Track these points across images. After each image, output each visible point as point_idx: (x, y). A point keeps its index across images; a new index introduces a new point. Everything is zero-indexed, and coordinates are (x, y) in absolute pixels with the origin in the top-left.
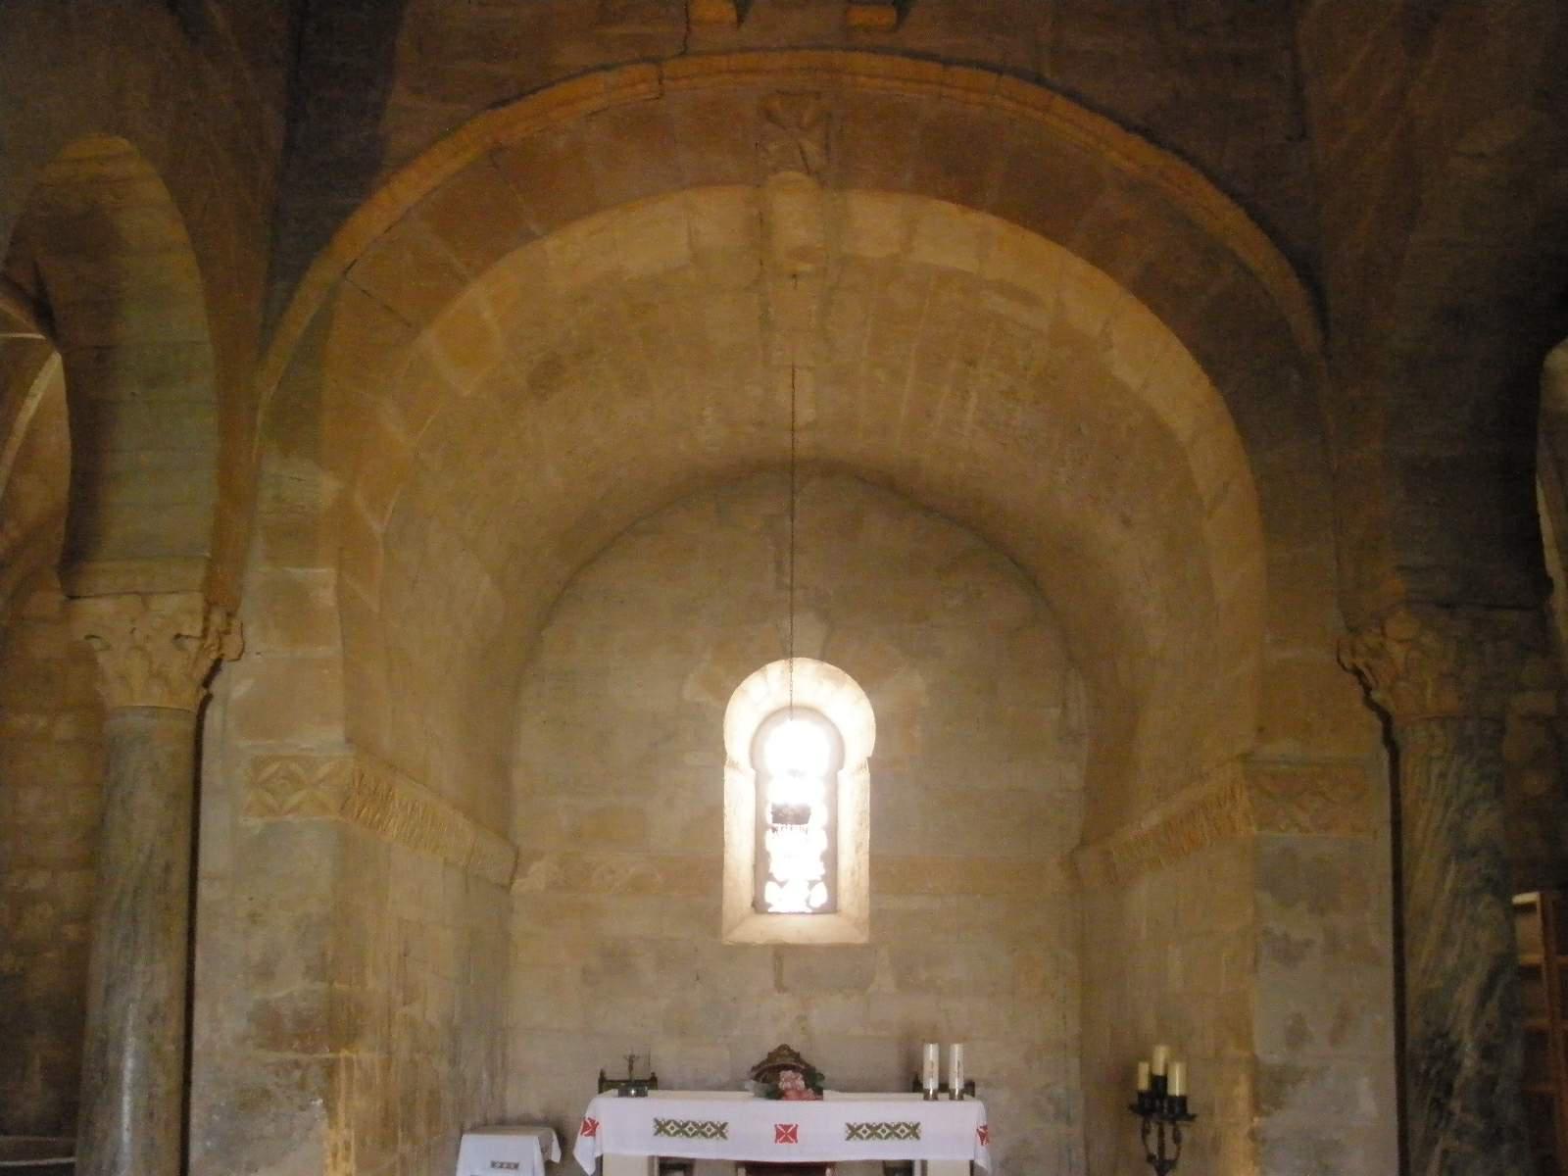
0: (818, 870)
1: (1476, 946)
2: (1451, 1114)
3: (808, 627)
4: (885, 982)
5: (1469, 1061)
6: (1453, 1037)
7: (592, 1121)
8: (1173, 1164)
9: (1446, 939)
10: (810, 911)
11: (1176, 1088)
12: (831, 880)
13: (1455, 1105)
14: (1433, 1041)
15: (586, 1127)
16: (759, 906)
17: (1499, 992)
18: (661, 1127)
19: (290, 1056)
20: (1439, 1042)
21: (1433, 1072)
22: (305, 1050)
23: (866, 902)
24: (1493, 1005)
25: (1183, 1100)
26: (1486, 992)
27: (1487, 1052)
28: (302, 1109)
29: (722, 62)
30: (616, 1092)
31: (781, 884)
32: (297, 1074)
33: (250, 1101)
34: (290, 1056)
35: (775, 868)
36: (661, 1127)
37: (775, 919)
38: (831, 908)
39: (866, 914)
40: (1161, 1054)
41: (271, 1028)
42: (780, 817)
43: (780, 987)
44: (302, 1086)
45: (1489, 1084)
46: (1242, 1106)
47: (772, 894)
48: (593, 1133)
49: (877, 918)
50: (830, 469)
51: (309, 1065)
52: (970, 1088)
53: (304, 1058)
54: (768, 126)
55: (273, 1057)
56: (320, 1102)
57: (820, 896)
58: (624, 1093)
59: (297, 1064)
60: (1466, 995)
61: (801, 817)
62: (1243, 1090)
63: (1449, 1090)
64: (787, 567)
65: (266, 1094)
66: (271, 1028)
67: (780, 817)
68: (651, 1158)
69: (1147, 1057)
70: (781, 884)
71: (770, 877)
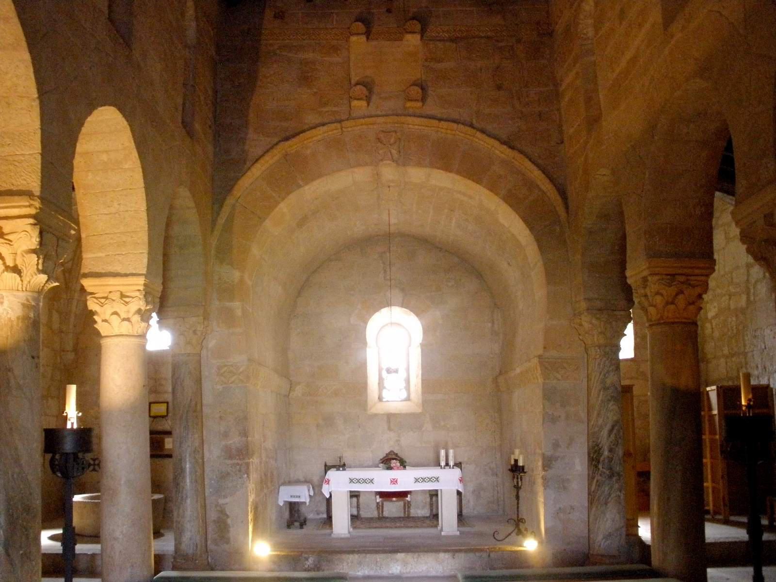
0: (403, 385)
1: (608, 418)
2: (599, 469)
3: (397, 294)
4: (428, 426)
5: (606, 453)
6: (600, 446)
7: (328, 480)
8: (520, 488)
9: (598, 415)
10: (400, 400)
11: (520, 464)
12: (408, 388)
13: (600, 466)
14: (595, 447)
15: (326, 482)
16: (380, 399)
17: (615, 431)
18: (351, 481)
19: (235, 461)
20: (596, 448)
21: (594, 457)
22: (240, 459)
23: (420, 397)
24: (613, 436)
25: (523, 467)
26: (611, 431)
27: (611, 450)
28: (240, 478)
29: (362, 121)
30: (335, 469)
31: (389, 390)
32: (238, 467)
33: (224, 476)
34: (235, 461)
35: (386, 384)
36: (351, 481)
37: (387, 403)
38: (408, 399)
39: (420, 401)
40: (517, 452)
41: (229, 453)
42: (389, 371)
43: (390, 429)
44: (240, 471)
45: (611, 460)
46: (540, 468)
47: (386, 395)
48: (328, 483)
49: (425, 402)
50: (402, 235)
51: (242, 464)
52: (458, 465)
53: (239, 462)
54: (379, 144)
55: (229, 462)
56: (246, 475)
57: (404, 395)
58: (338, 470)
59: (238, 464)
60: (605, 432)
61: (396, 371)
62: (540, 463)
63: (599, 462)
64: (388, 273)
65: (228, 474)
66: (229, 453)
67: (389, 371)
68: (348, 491)
69: (513, 453)
70: (389, 390)
71: (384, 388)
